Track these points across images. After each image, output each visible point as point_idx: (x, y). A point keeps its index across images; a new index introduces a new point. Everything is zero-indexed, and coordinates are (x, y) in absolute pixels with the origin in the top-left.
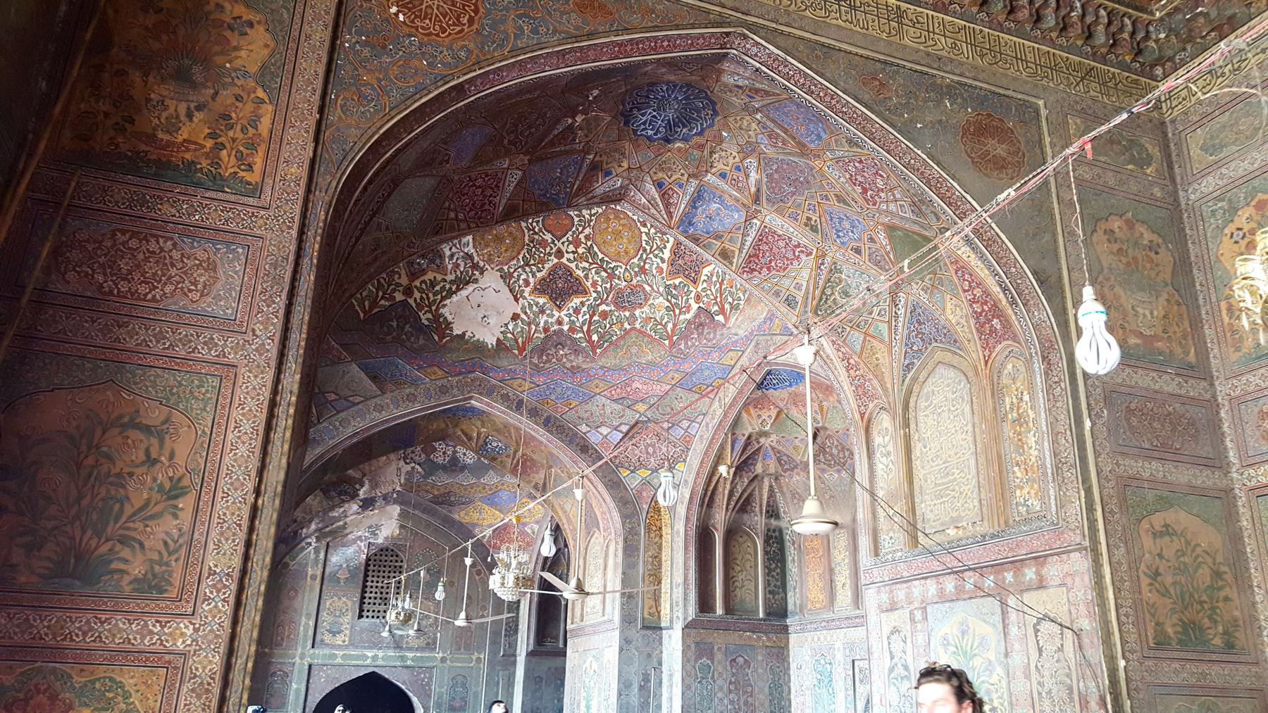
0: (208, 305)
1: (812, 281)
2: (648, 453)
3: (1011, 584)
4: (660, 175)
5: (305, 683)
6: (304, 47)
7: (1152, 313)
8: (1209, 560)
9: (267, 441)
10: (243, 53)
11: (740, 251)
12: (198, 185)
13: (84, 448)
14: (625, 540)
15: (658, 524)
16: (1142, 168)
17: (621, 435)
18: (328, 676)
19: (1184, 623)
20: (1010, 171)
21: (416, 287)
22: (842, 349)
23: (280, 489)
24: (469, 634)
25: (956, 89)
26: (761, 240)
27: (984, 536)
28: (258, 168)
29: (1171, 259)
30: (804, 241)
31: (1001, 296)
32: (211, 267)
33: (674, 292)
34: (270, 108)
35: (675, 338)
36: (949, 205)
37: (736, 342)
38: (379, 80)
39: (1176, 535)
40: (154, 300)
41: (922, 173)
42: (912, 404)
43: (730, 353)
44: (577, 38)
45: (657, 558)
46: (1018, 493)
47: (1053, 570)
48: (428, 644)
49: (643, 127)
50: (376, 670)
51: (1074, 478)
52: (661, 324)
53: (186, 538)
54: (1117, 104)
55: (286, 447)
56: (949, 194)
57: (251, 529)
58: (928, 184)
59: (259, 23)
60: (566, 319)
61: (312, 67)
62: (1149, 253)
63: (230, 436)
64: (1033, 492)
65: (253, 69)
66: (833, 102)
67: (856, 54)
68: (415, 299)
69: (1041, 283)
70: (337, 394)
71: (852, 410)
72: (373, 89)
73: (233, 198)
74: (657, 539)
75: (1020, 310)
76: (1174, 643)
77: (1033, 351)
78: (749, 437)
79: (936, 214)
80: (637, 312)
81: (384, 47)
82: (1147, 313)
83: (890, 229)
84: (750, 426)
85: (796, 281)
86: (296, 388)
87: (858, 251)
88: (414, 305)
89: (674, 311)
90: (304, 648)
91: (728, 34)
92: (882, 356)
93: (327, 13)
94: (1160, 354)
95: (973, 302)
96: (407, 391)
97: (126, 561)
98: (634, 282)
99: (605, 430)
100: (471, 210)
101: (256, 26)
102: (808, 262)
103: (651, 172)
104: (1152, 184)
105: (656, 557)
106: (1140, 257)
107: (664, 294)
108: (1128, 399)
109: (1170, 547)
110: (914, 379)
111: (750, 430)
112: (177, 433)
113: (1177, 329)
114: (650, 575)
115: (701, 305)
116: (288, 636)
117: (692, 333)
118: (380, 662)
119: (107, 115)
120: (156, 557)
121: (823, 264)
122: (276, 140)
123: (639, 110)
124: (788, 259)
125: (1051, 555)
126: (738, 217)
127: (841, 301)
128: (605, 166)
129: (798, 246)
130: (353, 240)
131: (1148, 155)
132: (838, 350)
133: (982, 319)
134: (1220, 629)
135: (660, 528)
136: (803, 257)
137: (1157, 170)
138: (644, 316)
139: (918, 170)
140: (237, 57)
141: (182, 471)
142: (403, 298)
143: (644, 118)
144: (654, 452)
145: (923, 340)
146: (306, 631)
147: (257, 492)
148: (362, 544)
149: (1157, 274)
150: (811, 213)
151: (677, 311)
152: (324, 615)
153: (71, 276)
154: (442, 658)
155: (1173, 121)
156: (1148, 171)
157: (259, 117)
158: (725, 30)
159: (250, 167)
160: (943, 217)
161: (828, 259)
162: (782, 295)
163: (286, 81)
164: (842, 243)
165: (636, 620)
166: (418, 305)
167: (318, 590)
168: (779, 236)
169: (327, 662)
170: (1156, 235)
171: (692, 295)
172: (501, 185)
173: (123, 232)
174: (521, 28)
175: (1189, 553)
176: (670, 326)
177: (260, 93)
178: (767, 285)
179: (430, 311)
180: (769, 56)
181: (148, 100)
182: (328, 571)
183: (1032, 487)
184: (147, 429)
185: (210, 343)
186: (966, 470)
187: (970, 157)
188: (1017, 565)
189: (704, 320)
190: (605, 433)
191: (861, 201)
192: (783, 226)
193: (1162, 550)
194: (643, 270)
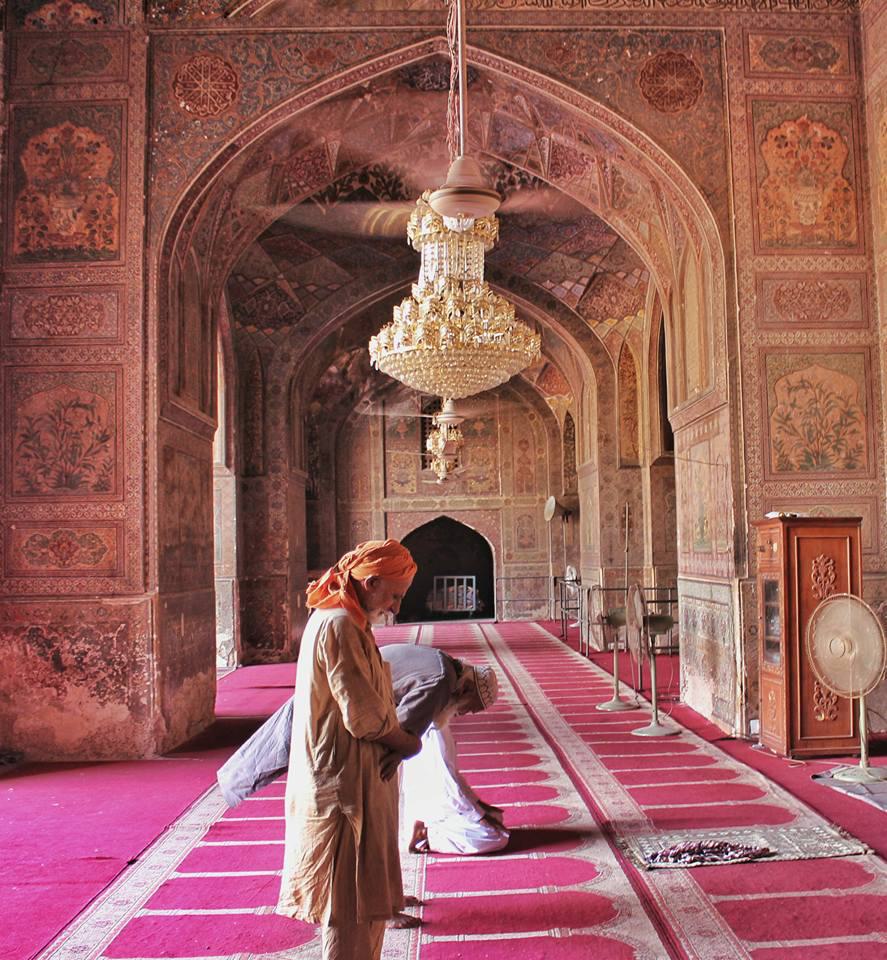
0: (103, 332)
1: (603, 183)
2: (611, 303)
5: (383, 530)
6: (131, 150)
7: (815, 204)
8: (841, 404)
9: (145, 404)
10: (97, 166)
12: (86, 259)
13: (58, 421)
15: (631, 370)
17: (583, 288)
18: (402, 522)
19: (807, 453)
20: (686, 102)
21: (371, 172)
23: (156, 430)
24: (530, 476)
25: (636, 36)
28: (115, 241)
29: (845, 150)
32: (100, 308)
34: (117, 199)
36: (632, 141)
38: (178, 159)
39: (811, 386)
40: (76, 334)
44: (308, 85)
48: (491, 488)
50: (446, 514)
53: (113, 462)
55: (156, 406)
56: (630, 133)
57: (145, 454)
58: (613, 125)
59: (103, 142)
60: (518, 179)
61: (137, 164)
62: (821, 149)
63: (126, 405)
65: (104, 175)
66: (525, 75)
67: (543, 30)
68: (372, 185)
69: (707, 196)
70: (316, 286)
72: (176, 167)
73: (105, 263)
74: (632, 384)
76: (796, 470)
81: (180, 133)
82: (811, 205)
86: (155, 371)
88: (371, 190)
90: (377, 498)
91: (431, 43)
93: (141, 122)
94: (819, 239)
96: (378, 272)
97: (86, 476)
99: (568, 284)
100: (308, 177)
101: (102, 145)
102: (594, 166)
104: (833, 82)
105: (631, 401)
108: (780, 283)
109: (803, 398)
112: (99, 406)
113: (840, 215)
114: (626, 419)
116: (362, 489)
118: (448, 507)
119: (33, 228)
120: (101, 473)
121: (606, 167)
122: (123, 219)
126: (530, 136)
127: (629, 196)
128: (411, 116)
130: (215, 233)
134: (843, 455)
135: (634, 374)
136: (590, 163)
140: (94, 170)
141: (105, 427)
142: (360, 186)
143: (425, 80)
144: (617, 301)
146: (377, 482)
147: (145, 434)
148: (415, 399)
149: (827, 168)
152: (390, 466)
153: (34, 328)
154: (506, 501)
157: (111, 207)
159: (111, 242)
163: (123, 175)
165: (614, 460)
166: (375, 189)
167: (382, 446)
169: (399, 510)
170: (831, 131)
172: (326, 153)
173: (54, 297)
174: (268, 90)
175: (822, 400)
177: (110, 191)
179: (388, 193)
181: (52, 213)
182: (388, 426)
184: (85, 407)
185: (107, 354)
187: (646, 97)
190: (569, 288)
193: (795, 400)
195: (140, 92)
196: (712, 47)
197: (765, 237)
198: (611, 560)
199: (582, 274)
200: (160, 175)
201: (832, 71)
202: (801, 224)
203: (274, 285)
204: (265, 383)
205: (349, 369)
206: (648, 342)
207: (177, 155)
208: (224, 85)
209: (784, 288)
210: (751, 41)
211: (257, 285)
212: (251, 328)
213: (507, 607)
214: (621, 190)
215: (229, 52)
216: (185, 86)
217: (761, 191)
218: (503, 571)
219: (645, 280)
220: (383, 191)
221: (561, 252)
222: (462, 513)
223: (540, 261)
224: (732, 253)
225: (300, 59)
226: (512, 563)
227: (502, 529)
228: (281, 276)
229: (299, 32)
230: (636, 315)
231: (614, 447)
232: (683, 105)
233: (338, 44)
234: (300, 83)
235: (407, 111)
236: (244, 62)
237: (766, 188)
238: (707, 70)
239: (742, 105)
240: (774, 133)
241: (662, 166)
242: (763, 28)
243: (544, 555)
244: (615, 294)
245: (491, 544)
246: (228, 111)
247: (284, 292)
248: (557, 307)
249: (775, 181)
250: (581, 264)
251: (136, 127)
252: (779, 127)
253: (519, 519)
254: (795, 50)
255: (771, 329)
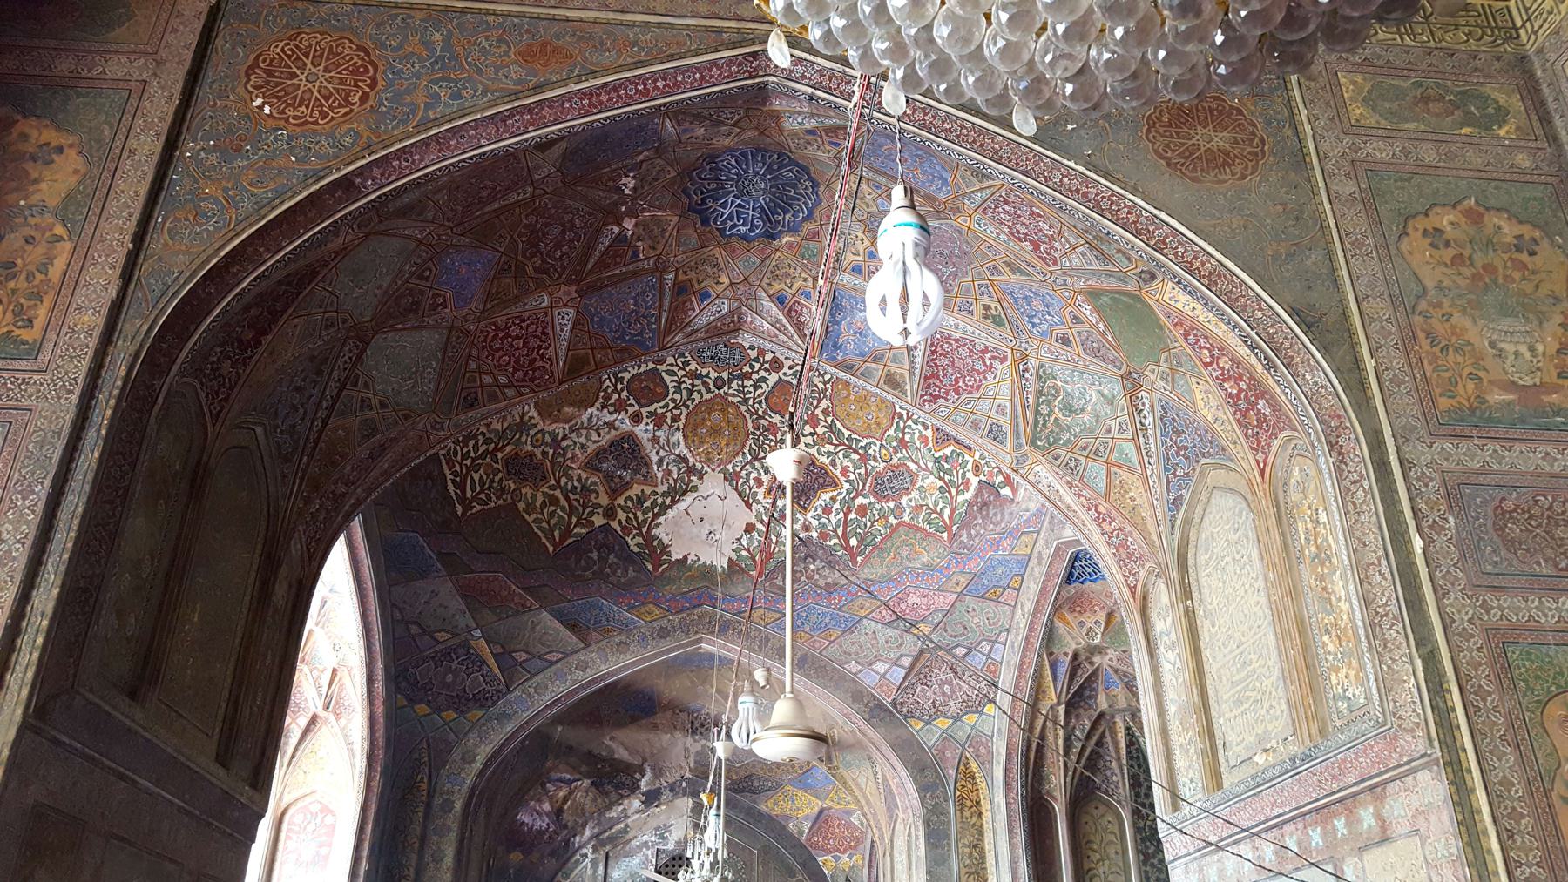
1: (1017, 399)
2: (944, 694)
3: (1345, 840)
4: (777, 286)
6: (126, 165)
7: (1532, 349)
10: (44, 186)
11: (912, 374)
14: (927, 823)
16: (1489, 129)
17: (903, 672)
20: (1238, 169)
21: (619, 506)
22: (1084, 493)
26: (934, 352)
27: (1293, 760)
28: (39, 323)
30: (991, 342)
31: (1253, 360)
33: (946, 466)
35: (954, 528)
37: (1028, 520)
38: (226, 190)
41: (1085, 194)
42: (1190, 562)
43: (1023, 537)
44: (517, 95)
45: (977, 846)
46: (1333, 677)
47: (1399, 806)
49: (730, 223)
51: (1401, 639)
52: (935, 512)
54: (1432, 44)
56: (1132, 218)
59: (71, 146)
60: (815, 523)
62: (1516, 255)
64: (1352, 673)
65: (53, 202)
66: (928, 118)
68: (620, 522)
69: (1307, 327)
70: (527, 653)
71: (1117, 584)
72: (217, 201)
75: (1283, 375)
77: (1313, 437)
78: (1076, 656)
79: (1124, 254)
80: (904, 501)
82: (1523, 349)
83: (1093, 295)
84: (1071, 640)
85: (996, 403)
87: (1065, 340)
89: (949, 492)
92: (1136, 491)
93: (161, 119)
95: (1222, 379)
96: (617, 640)
98: (895, 461)
99: (881, 667)
100: (515, 370)
102: (1004, 370)
103: (764, 284)
104: (1510, 150)
105: (975, 846)
106: (1498, 263)
107: (935, 472)
110: (1187, 522)
111: (1074, 646)
114: (970, 874)
115: (982, 477)
117: (975, 518)
121: (1026, 370)
123: (715, 200)
124: (979, 373)
125: (1392, 780)
127: (1066, 420)
128: (696, 287)
129: (985, 351)
130: (319, 423)
131: (1499, 109)
132: (1080, 495)
133: (1243, 404)
135: (978, 803)
136: (996, 364)
137: (1518, 129)
138: (913, 504)
139: (1077, 191)
142: (605, 521)
143: (727, 212)
144: (953, 692)
145: (1187, 458)
148: (649, 852)
150: (986, 300)
151: (954, 491)
155: (1540, 51)
156: (1502, 133)
158: (748, 50)
160: (1132, 253)
161: (1032, 362)
162: (982, 425)
164: (1042, 334)
166: (624, 528)
168: (957, 341)
171: (969, 466)
172: (549, 330)
176: (947, 512)
178: (959, 416)
180: (821, 72)
183: (1350, 664)
186: (1265, 652)
188: (1347, 803)
189: (989, 497)
191: (1039, 264)
192: (957, 325)
194: (903, 444)
195: (175, 77)
196: (1272, 91)
197: (1444, 403)
199: (902, 651)
200: (180, 214)
201: (1502, 133)
202: (1513, 383)
203: (466, 645)
204: (430, 796)
205: (566, 807)
206: (1003, 752)
207: (224, 183)
208: (350, 79)
209: (1508, 504)
210: (1343, 80)
211: (438, 642)
212: (422, 709)
214: (1051, 411)
215: (371, 30)
216: (270, 74)
217: (1417, 319)
219: (998, 658)
220: (635, 532)
224: (1378, 432)
225: (506, 53)
228: (478, 633)
229: (509, 14)
230: (981, 713)
232: (1233, 174)
233: (581, 38)
234: (502, 90)
235: (692, 275)
236: (394, 49)
237: (1426, 316)
238: (1269, 123)
239: (1347, 175)
240: (1421, 223)
241: (1200, 279)
242: (1361, 65)
246: (350, 121)
247: (478, 656)
249: (1439, 305)
250: (901, 637)
251: (147, 126)
252: (1427, 215)
254: (1425, 99)
255: (1502, 589)
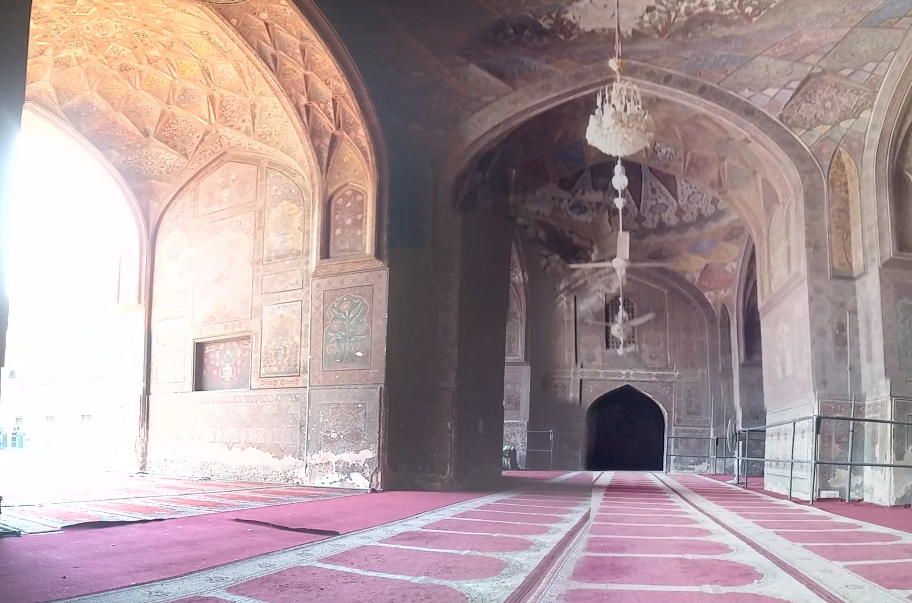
2: (825, 108)
14: (806, 194)
15: (843, 180)
17: (791, 93)
18: (595, 388)
45: (844, 210)
74: (843, 194)
99: (771, 92)
105: (843, 211)
118: (632, 378)
144: (833, 106)
165: (825, 270)
169: (593, 378)
190: (772, 95)
198: (825, 383)
199: (792, 76)
213: (675, 461)
218: (673, 432)
221: (767, 55)
222: (643, 383)
223: (738, 68)
226: (681, 426)
227: (674, 399)
231: (825, 256)
243: (707, 422)
244: (831, 99)
245: (661, 406)
248: (757, 115)
253: (688, 391)
